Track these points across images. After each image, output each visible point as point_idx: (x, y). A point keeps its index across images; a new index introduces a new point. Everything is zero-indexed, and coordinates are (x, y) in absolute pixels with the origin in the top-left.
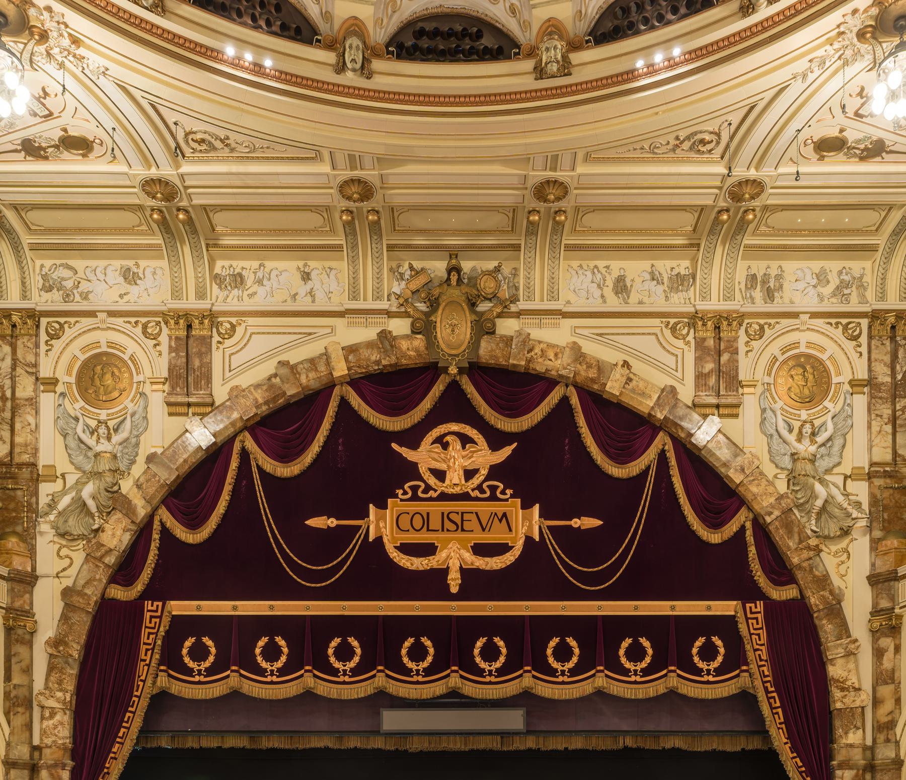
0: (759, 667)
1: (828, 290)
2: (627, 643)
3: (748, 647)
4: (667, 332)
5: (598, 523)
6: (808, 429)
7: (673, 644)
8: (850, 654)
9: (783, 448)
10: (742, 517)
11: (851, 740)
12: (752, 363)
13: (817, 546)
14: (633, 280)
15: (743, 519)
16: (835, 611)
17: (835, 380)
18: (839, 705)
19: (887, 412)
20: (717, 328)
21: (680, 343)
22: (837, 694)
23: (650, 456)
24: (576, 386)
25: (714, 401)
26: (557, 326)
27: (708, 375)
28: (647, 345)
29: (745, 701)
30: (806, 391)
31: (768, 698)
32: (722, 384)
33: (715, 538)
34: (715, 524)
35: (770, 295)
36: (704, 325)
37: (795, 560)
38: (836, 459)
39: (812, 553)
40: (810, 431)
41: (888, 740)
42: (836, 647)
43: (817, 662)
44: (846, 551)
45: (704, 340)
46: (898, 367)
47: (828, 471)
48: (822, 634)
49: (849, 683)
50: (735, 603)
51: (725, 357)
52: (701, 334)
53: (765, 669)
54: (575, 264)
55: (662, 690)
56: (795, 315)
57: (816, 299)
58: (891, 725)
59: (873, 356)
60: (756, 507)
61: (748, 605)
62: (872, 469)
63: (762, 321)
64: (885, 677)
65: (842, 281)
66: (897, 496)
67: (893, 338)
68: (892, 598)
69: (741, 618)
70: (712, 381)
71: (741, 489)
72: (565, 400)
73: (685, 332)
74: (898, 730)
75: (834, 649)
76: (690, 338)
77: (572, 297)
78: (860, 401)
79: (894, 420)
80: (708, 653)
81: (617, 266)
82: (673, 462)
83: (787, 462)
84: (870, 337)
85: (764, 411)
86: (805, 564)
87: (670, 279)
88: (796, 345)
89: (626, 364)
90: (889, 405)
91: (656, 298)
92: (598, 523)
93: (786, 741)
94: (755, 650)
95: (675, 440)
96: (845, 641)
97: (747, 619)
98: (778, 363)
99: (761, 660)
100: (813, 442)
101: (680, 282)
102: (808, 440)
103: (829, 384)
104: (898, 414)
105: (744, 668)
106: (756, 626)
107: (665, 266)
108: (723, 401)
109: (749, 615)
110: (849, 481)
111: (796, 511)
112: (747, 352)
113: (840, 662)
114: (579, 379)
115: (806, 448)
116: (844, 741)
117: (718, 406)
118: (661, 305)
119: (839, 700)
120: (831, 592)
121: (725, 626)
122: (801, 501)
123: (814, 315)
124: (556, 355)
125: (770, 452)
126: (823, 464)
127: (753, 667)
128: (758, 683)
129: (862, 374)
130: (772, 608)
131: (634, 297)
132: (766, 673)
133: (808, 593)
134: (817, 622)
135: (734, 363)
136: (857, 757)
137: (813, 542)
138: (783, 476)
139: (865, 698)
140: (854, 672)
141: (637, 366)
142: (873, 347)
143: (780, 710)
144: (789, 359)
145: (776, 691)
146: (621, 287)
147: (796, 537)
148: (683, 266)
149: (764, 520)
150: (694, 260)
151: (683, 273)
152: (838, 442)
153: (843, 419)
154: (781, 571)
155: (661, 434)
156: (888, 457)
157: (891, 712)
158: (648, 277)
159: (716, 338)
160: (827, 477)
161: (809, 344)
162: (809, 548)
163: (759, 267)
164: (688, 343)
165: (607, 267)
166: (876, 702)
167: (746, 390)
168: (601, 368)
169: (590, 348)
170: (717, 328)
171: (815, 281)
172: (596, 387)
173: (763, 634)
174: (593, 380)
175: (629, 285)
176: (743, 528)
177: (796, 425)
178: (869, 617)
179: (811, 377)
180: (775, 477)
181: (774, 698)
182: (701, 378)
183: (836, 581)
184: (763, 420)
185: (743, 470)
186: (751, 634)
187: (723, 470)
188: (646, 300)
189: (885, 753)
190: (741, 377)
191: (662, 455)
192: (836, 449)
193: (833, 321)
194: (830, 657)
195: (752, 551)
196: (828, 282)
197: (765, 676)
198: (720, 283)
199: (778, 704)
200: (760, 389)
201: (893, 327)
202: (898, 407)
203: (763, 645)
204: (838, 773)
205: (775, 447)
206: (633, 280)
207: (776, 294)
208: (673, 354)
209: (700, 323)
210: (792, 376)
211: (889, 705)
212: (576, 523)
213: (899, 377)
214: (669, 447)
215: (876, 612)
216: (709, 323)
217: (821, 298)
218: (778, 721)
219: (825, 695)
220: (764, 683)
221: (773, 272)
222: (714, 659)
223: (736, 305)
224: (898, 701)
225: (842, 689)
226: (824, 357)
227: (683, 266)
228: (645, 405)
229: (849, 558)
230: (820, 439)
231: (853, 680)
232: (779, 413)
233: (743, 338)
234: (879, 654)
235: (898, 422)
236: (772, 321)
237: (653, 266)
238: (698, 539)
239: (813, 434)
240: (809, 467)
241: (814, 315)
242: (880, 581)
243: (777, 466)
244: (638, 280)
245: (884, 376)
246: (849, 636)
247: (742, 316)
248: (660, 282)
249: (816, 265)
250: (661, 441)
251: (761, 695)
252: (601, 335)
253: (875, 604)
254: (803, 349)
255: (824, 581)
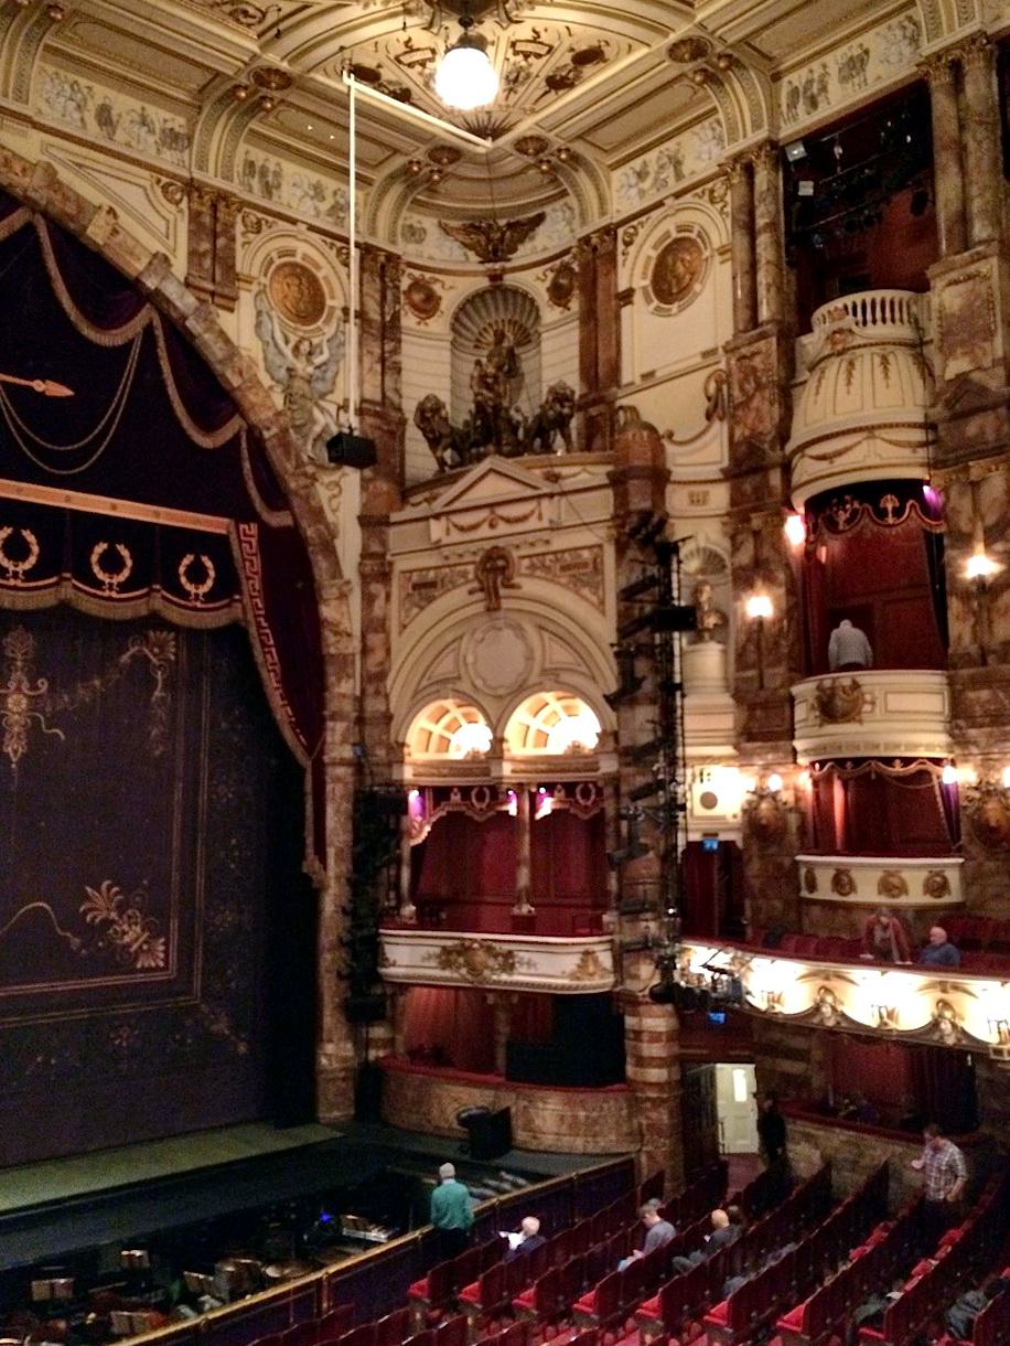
0: (252, 597)
1: (324, 206)
2: (101, 548)
3: (243, 576)
4: (158, 190)
5: (68, 392)
6: (305, 347)
7: (157, 555)
8: (343, 596)
9: (278, 360)
10: (234, 426)
11: (343, 690)
12: (249, 259)
13: (314, 474)
14: (120, 115)
15: (237, 427)
16: (329, 549)
17: (329, 302)
18: (332, 650)
19: (377, 351)
20: (214, 207)
21: (172, 208)
22: (329, 637)
23: (133, 329)
24: (45, 214)
25: (210, 286)
26: (24, 135)
27: (204, 254)
28: (134, 196)
29: (234, 637)
30: (302, 306)
31: (260, 635)
32: (218, 276)
33: (206, 442)
34: (209, 427)
35: (268, 190)
36: (200, 197)
37: (293, 485)
38: (328, 386)
39: (308, 481)
40: (308, 349)
41: (377, 693)
42: (333, 586)
43: (309, 597)
44: (337, 484)
45: (199, 214)
46: (387, 309)
47: (323, 396)
48: (316, 571)
49: (342, 627)
50: (226, 520)
51: (221, 242)
52: (195, 206)
53: (258, 600)
54: (51, 69)
55: (144, 612)
56: (294, 222)
57: (313, 212)
58: (381, 676)
59: (365, 289)
60: (253, 418)
61: (242, 526)
62: (365, 405)
63: (260, 215)
64: (374, 625)
65: (337, 202)
66: (386, 438)
67: (382, 277)
68: (384, 543)
69: (233, 537)
70: (207, 263)
71: (238, 394)
72: (29, 228)
73: (178, 196)
74: (389, 682)
75: (329, 591)
76: (184, 205)
77: (45, 108)
78: (353, 329)
79: (383, 360)
80: (197, 574)
81: (102, 93)
82: (161, 343)
83: (282, 373)
84: (362, 269)
85: (259, 313)
86: (302, 492)
87: (163, 131)
88: (292, 253)
89: (111, 211)
90: (378, 344)
91: (148, 147)
92: (68, 392)
93: (275, 685)
94: (248, 578)
95: (166, 319)
96: (338, 582)
97: (240, 542)
98: (273, 267)
99: (254, 590)
100: (309, 362)
101: (172, 139)
102: (304, 359)
103: (322, 304)
104: (387, 355)
105: (237, 597)
106: (249, 551)
107: (158, 115)
108: (219, 290)
109: (243, 538)
110: (341, 412)
111: (291, 431)
112: (244, 244)
113: (334, 603)
114: (50, 208)
115: (301, 366)
116: (337, 690)
117: (213, 294)
118: (149, 156)
119: (333, 645)
120: (327, 526)
121: (216, 546)
122: (298, 423)
123: (312, 228)
124: (24, 170)
125: (265, 359)
126: (320, 386)
127: (246, 600)
128: (250, 616)
129: (354, 306)
130: (266, 531)
131: (120, 136)
132: (260, 605)
133: (304, 524)
134: (312, 557)
135: (230, 249)
136: (348, 707)
137: (310, 469)
138: (278, 389)
139: (356, 644)
140: (346, 616)
141: (125, 220)
142: (365, 281)
143: (273, 650)
144: (285, 265)
145: (269, 628)
146: (105, 117)
147: (294, 463)
148: (179, 123)
149: (261, 434)
150: (192, 124)
151: (177, 129)
152: (333, 368)
153: (337, 343)
154: (277, 495)
155: (148, 305)
156: (378, 397)
157: (381, 664)
158: (137, 118)
159: (213, 217)
160: (322, 403)
161: (305, 257)
162: (305, 474)
163: (259, 156)
164: (181, 211)
165: (89, 88)
166: (365, 651)
167: (242, 284)
168: (80, 202)
169: (65, 175)
170: (214, 207)
171: (312, 193)
172: (72, 226)
173: (257, 561)
174: (71, 218)
175: (115, 118)
176: (237, 437)
177: (293, 339)
178: (359, 560)
179: (306, 292)
180: (271, 388)
181: (267, 635)
182: (193, 254)
183: (330, 517)
184: (258, 325)
185: (241, 373)
186: (244, 560)
187: (219, 367)
188: (134, 143)
189: (374, 706)
190: (238, 268)
191: (149, 330)
192: (329, 375)
193: (329, 240)
194: (325, 597)
195: (247, 465)
196: (324, 199)
197: (259, 609)
198: (222, 155)
199: (272, 642)
200: (255, 288)
201: (383, 267)
202: (387, 348)
203: (256, 573)
204: (330, 724)
205: (270, 357)
206: (120, 115)
207: (274, 191)
208: (164, 218)
209: (196, 194)
210: (288, 285)
211: (379, 655)
212: (38, 386)
213: (388, 318)
214: (157, 322)
215: (366, 555)
216: (207, 198)
217: (318, 214)
218: (270, 660)
219: (318, 639)
220: (256, 616)
221: (272, 167)
222: (203, 582)
223: (233, 187)
224: (388, 651)
225: (336, 633)
226: (320, 275)
227: (179, 123)
228: (136, 266)
229: (340, 492)
230: (318, 360)
231: (345, 625)
232: (276, 321)
233: (239, 228)
234: (368, 599)
235: (387, 364)
236: (270, 219)
237: (143, 109)
238: (188, 439)
239: (310, 353)
240: (306, 387)
241: (312, 228)
242: (372, 523)
243: (273, 378)
244: (126, 119)
245: (375, 316)
246: (341, 577)
247: (244, 203)
248: (151, 131)
249: (316, 177)
250: (146, 315)
251: (253, 630)
252: (80, 166)
253: (365, 547)
254: (298, 259)
255: (318, 514)
